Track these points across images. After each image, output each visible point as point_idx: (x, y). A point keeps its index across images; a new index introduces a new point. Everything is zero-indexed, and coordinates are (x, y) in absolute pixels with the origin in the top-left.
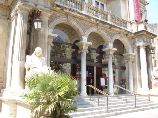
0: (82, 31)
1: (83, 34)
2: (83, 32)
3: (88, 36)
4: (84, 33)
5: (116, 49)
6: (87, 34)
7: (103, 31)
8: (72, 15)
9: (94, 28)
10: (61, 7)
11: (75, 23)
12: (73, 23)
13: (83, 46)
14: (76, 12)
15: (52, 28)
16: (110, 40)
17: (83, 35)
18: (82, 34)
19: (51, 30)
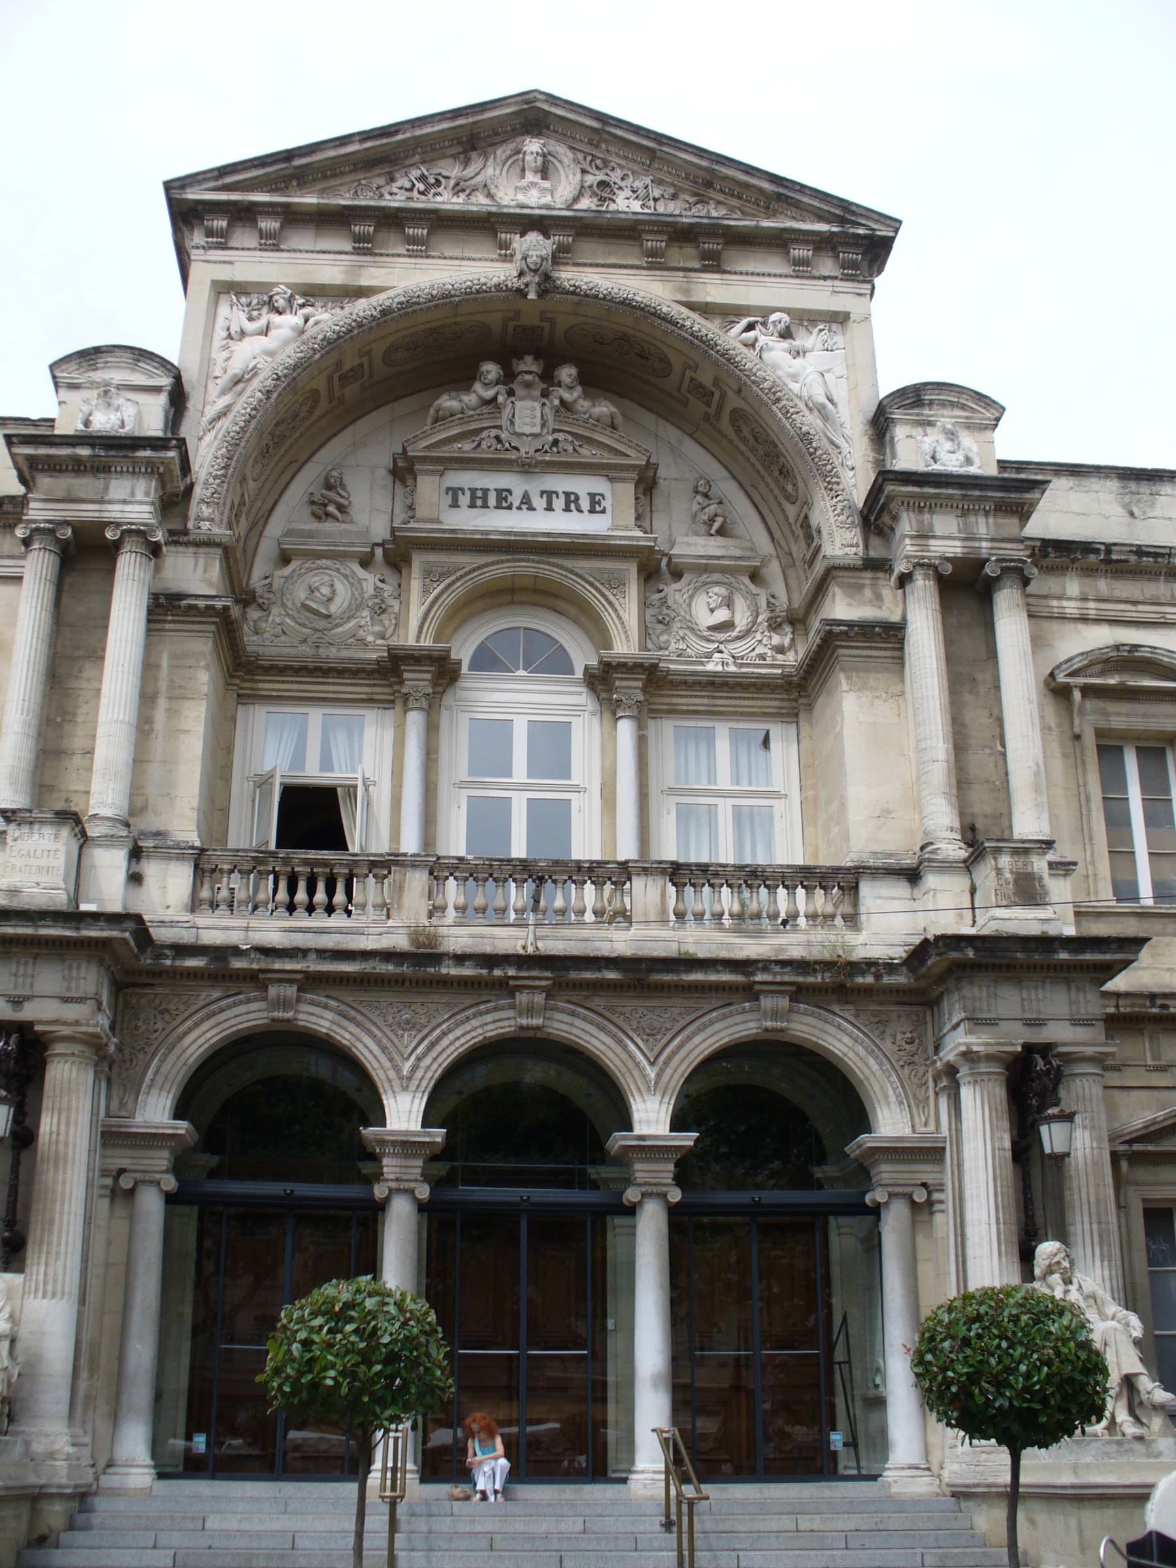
0: (383, 1059)
1: (390, 1081)
2: (388, 1064)
3: (428, 1084)
4: (392, 1074)
5: (688, 1139)
6: (419, 1074)
7: (578, 1023)
8: (286, 978)
9: (489, 1018)
10: (204, 955)
11: (330, 1015)
12: (314, 1019)
13: (385, 1161)
14: (312, 956)
15: (167, 1086)
16: (644, 1076)
17: (386, 1085)
18: (383, 1077)
19: (164, 1094)
